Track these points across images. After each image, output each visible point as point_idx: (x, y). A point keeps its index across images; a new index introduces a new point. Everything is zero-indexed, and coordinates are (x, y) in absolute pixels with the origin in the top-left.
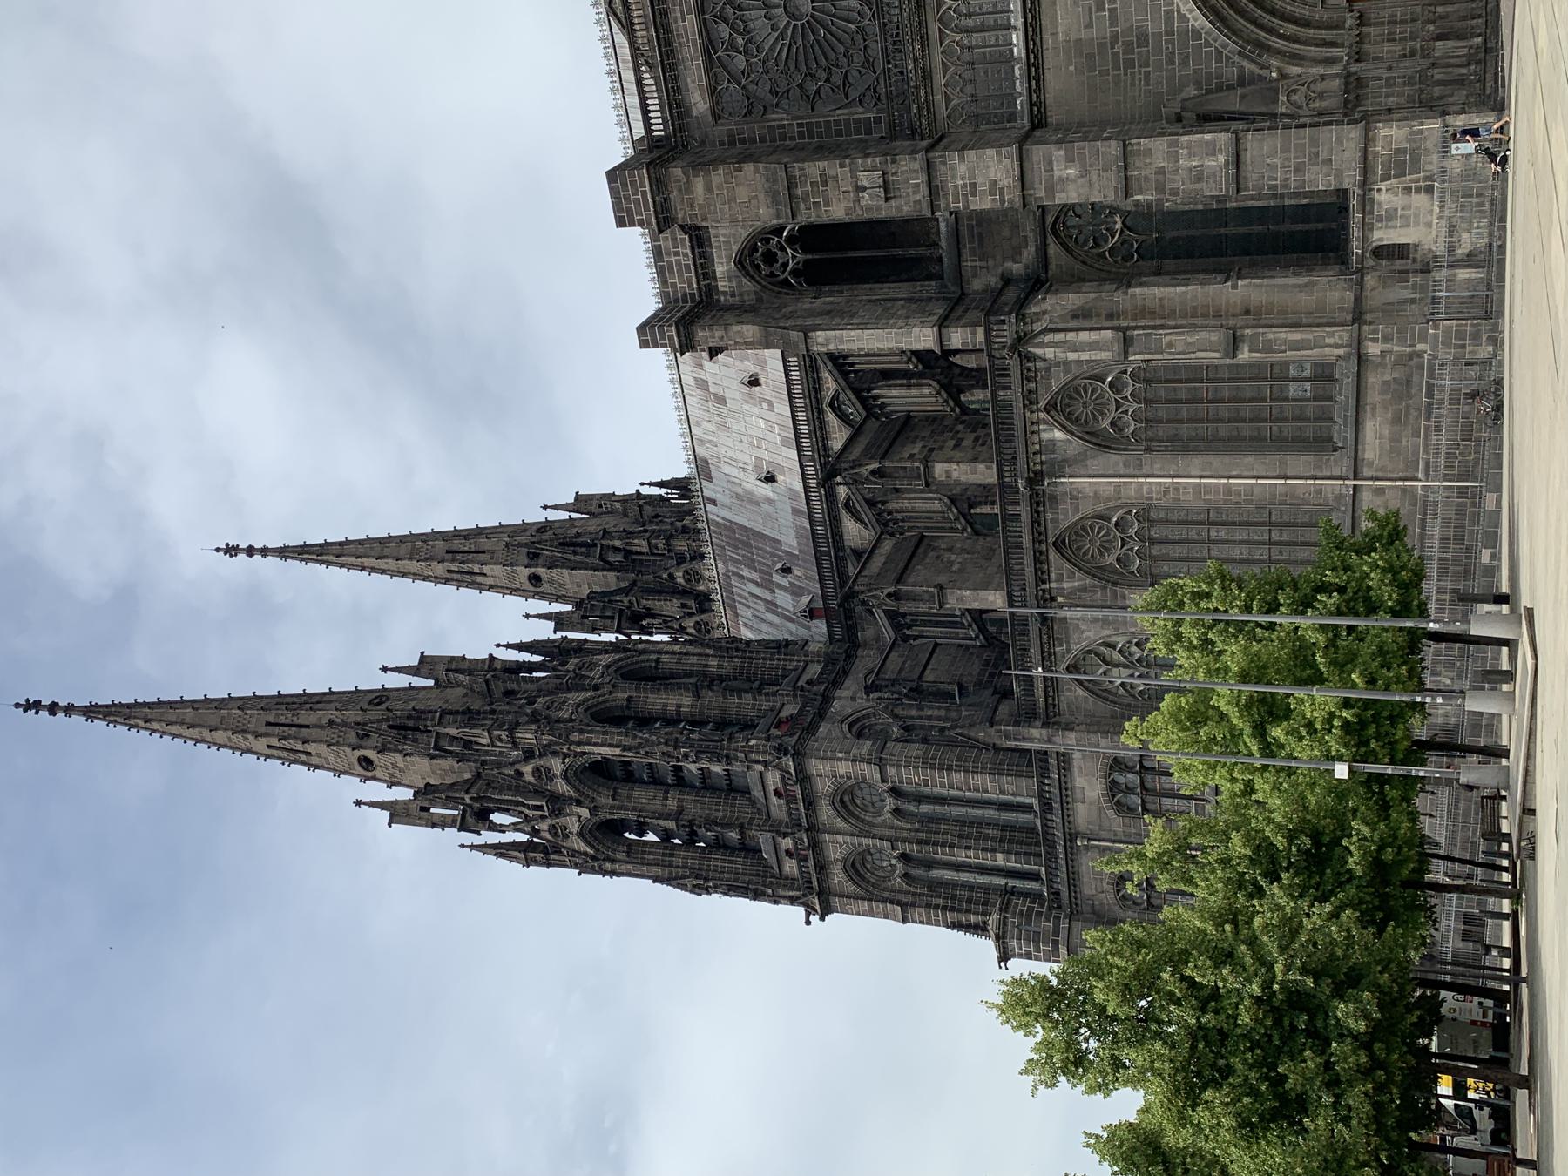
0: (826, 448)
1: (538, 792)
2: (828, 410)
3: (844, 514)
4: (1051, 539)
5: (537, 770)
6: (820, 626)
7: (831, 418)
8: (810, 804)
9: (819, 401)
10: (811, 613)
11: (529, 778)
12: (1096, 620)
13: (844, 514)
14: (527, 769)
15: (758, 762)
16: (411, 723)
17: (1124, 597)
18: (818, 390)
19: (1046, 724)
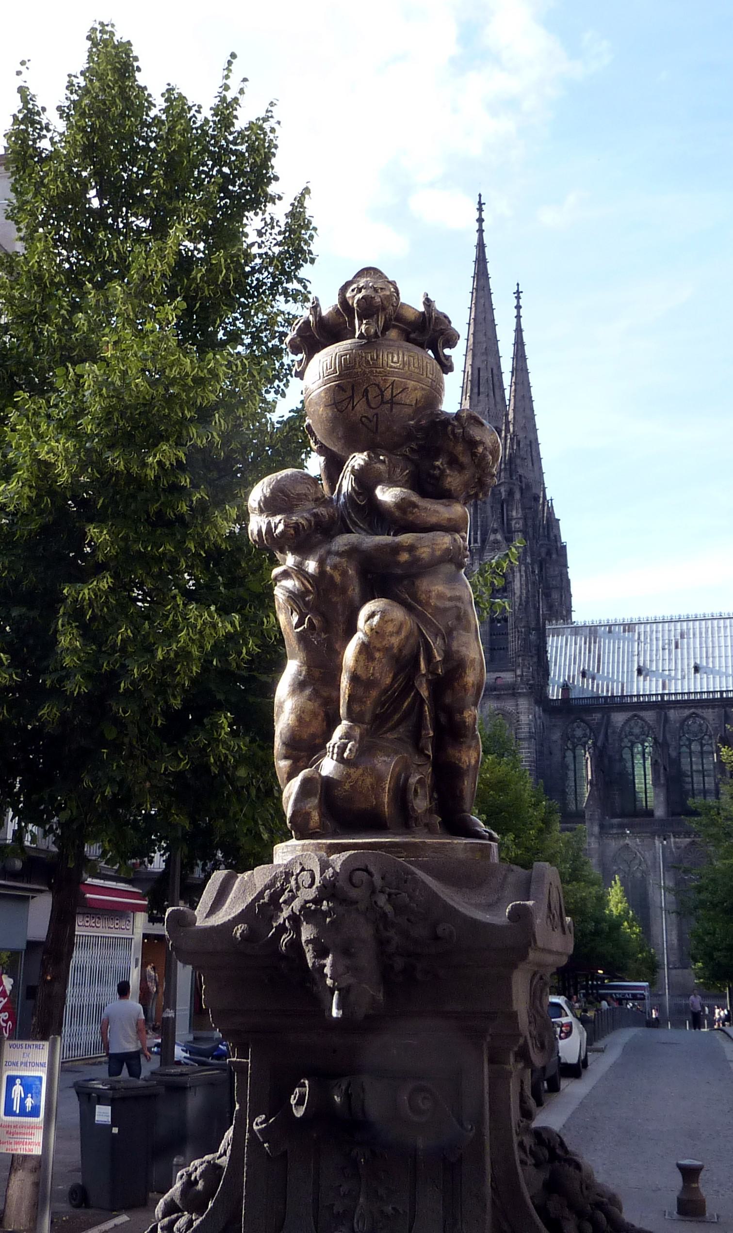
0: (670, 708)
1: (484, 541)
2: (692, 711)
3: (630, 714)
4: (696, 839)
5: (496, 542)
6: (554, 693)
7: (687, 712)
8: (498, 698)
9: (696, 707)
10: (566, 688)
11: (492, 537)
12: (655, 858)
13: (630, 714)
14: (499, 537)
15: (522, 672)
16: (513, 466)
17: (668, 871)
18: (702, 707)
19: (600, 833)
